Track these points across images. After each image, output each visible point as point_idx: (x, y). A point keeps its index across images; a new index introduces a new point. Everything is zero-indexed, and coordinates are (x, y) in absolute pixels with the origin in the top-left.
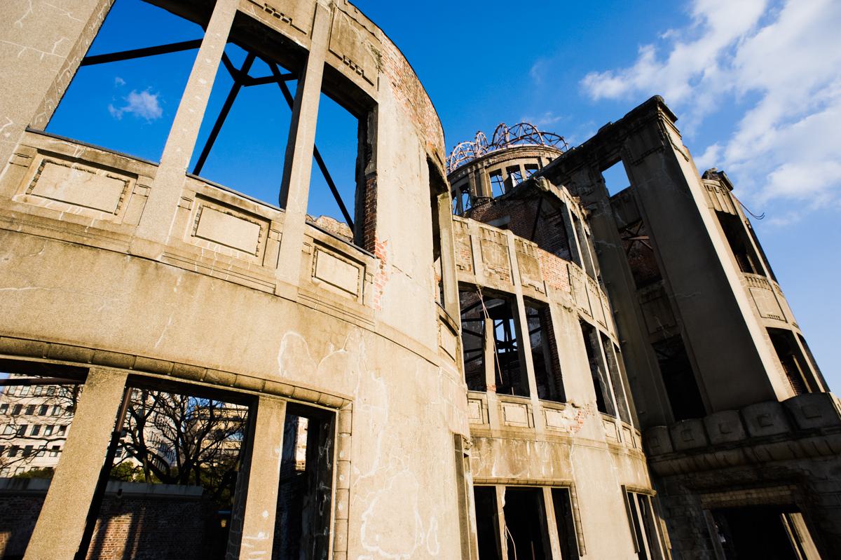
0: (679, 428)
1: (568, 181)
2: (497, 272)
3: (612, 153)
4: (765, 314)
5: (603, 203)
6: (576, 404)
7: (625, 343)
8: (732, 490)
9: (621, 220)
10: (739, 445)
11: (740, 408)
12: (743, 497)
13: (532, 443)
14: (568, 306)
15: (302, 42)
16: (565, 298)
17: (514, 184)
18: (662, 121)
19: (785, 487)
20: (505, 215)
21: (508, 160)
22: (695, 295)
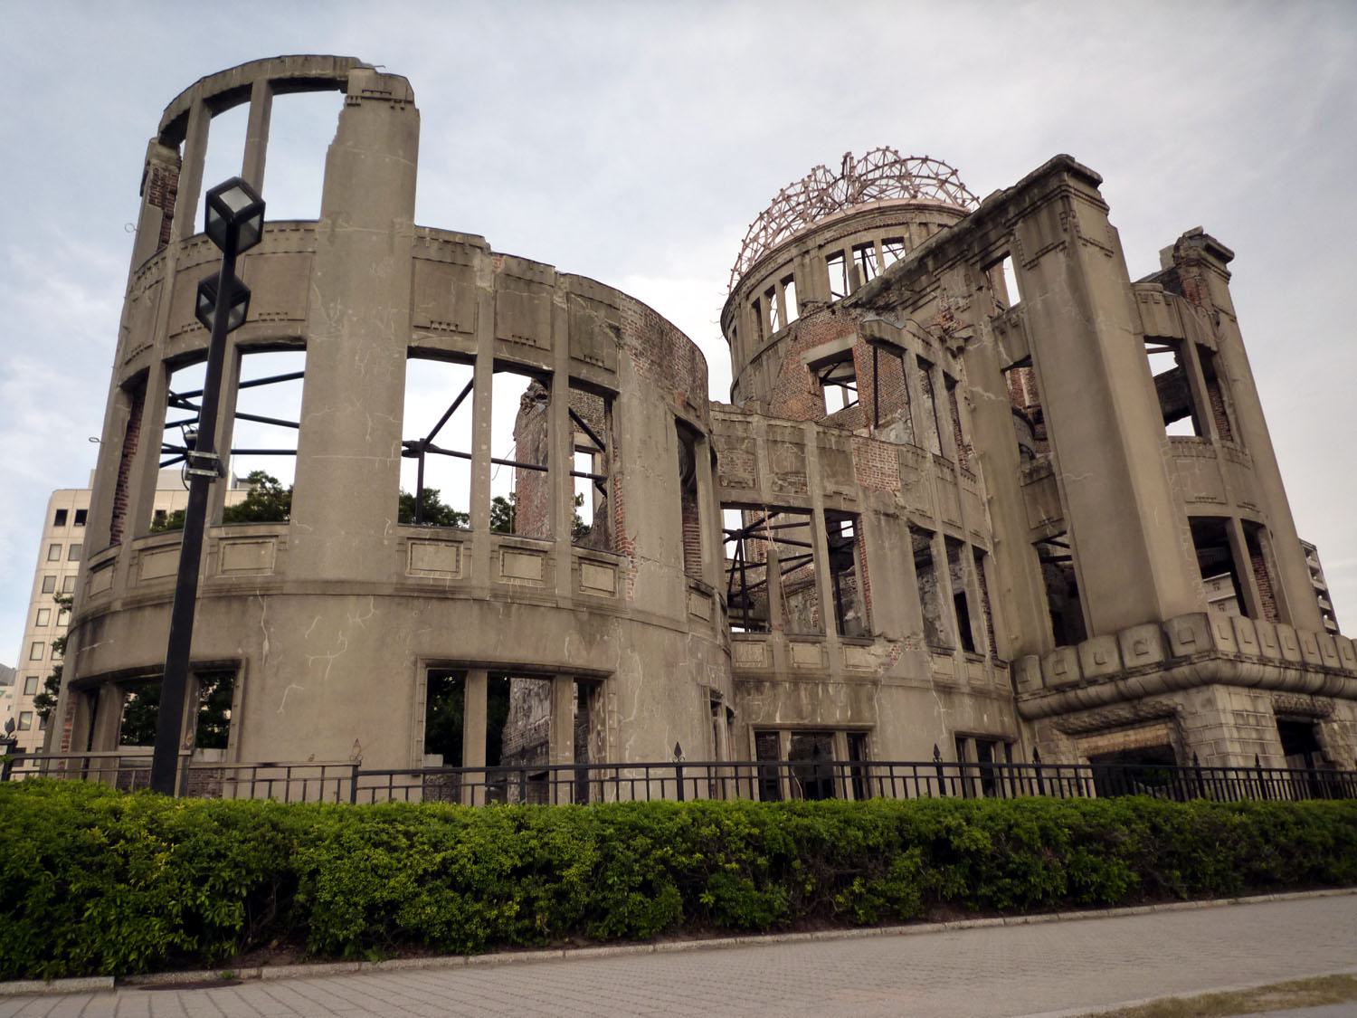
0: (1052, 658)
1: (936, 285)
2: (790, 483)
3: (998, 244)
4: (1192, 495)
5: (983, 327)
6: (891, 636)
7: (999, 542)
8: (1110, 733)
9: (1005, 356)
10: (1111, 678)
11: (1117, 635)
12: (1121, 740)
13: (825, 684)
14: (891, 511)
15: (547, 365)
16: (887, 501)
17: (863, 282)
18: (1067, 197)
19: (1163, 726)
20: (849, 333)
21: (856, 232)
22: (1085, 478)
